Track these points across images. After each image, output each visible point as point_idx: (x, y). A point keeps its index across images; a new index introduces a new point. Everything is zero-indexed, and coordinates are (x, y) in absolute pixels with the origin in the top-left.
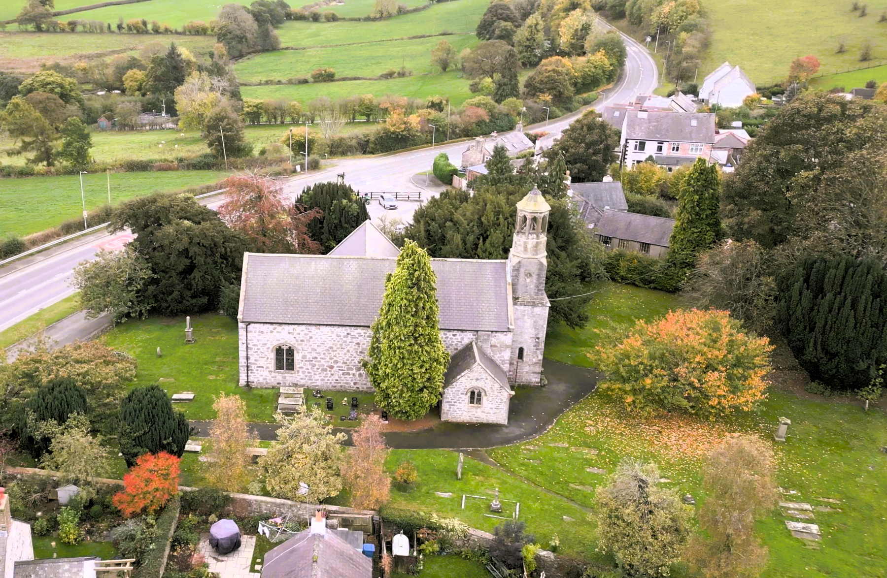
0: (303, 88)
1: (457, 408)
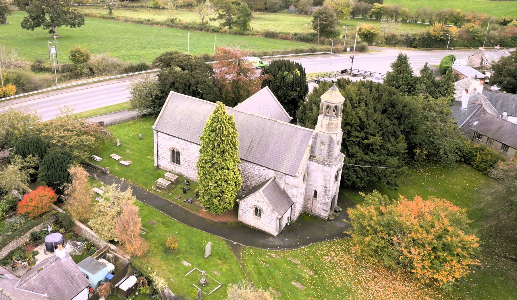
1: (247, 216)
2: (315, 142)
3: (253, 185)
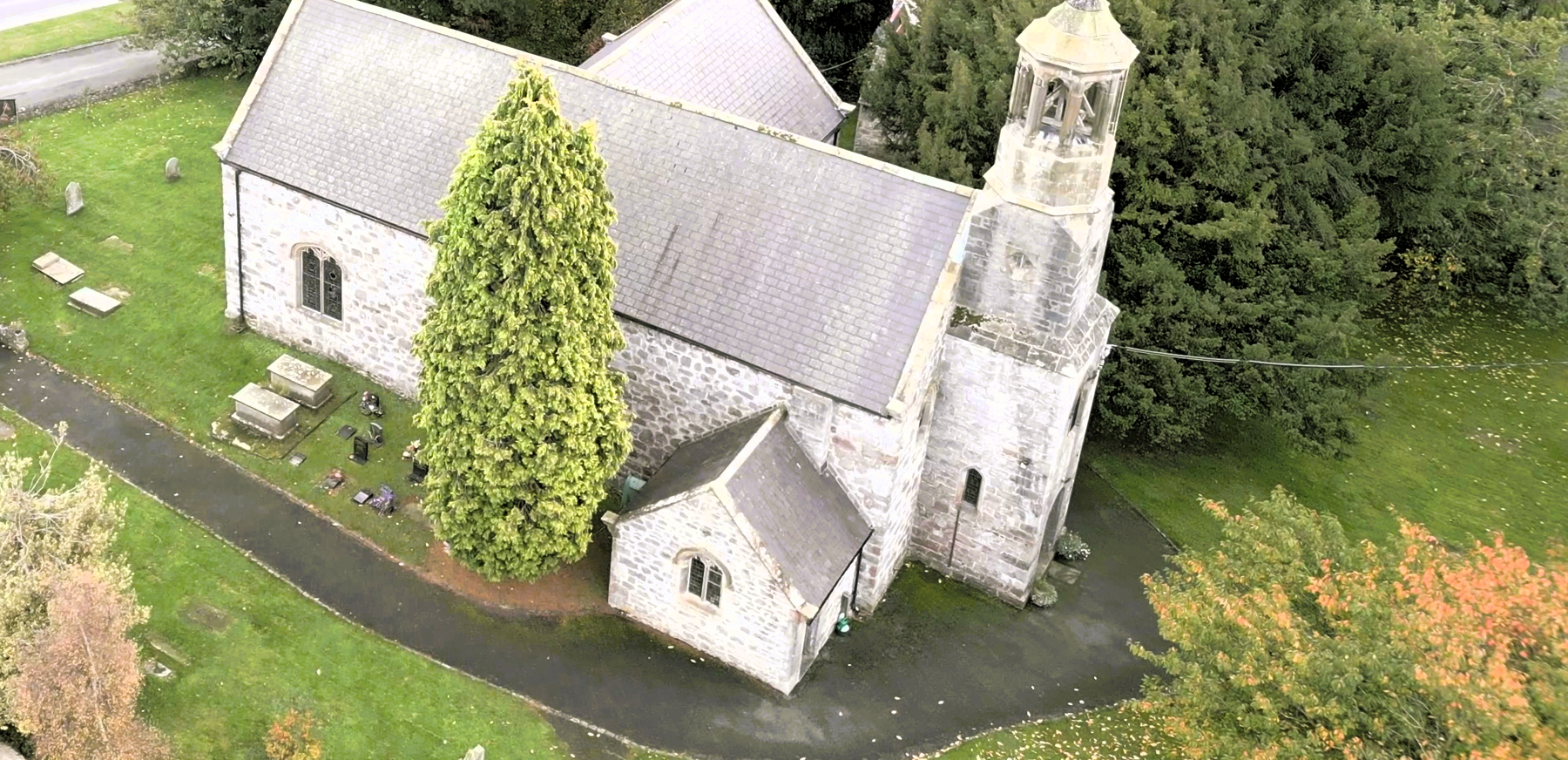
2: (979, 251)
3: (680, 436)
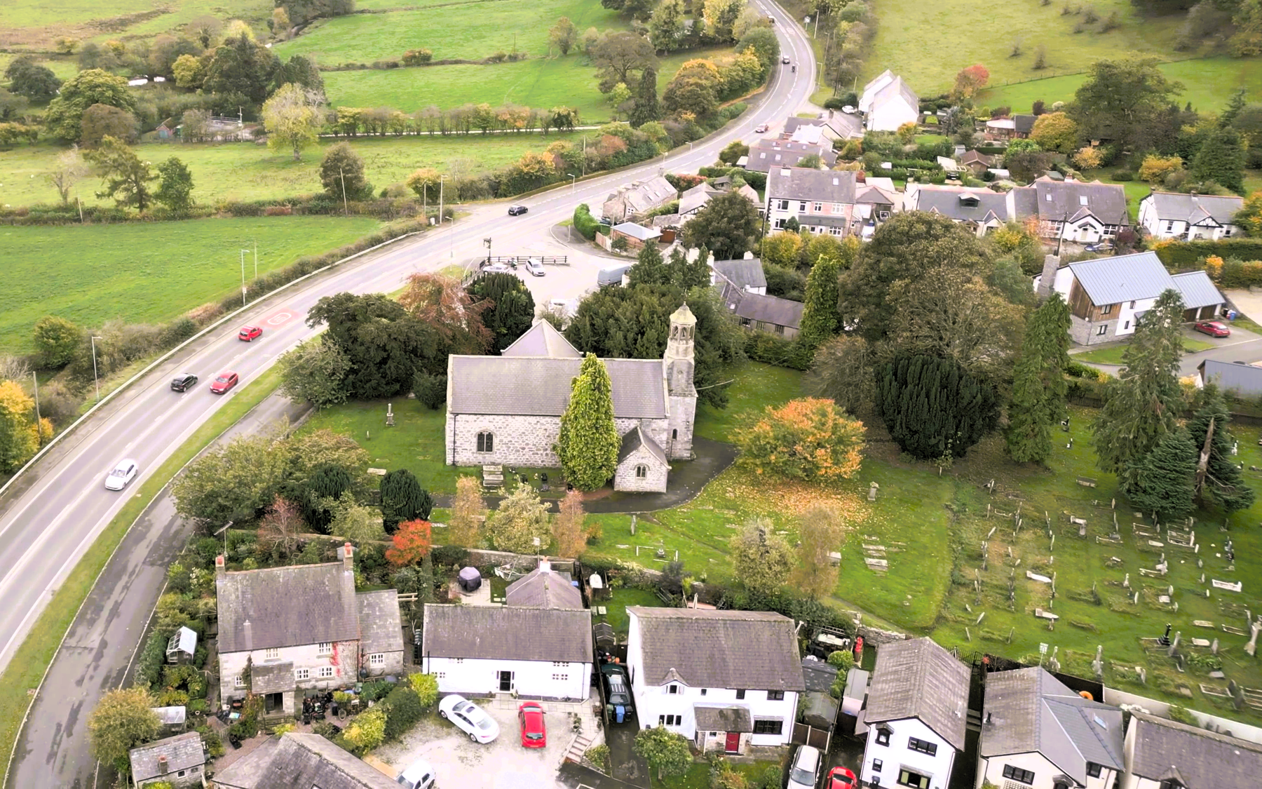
0: (393, 75)
1: (627, 480)
